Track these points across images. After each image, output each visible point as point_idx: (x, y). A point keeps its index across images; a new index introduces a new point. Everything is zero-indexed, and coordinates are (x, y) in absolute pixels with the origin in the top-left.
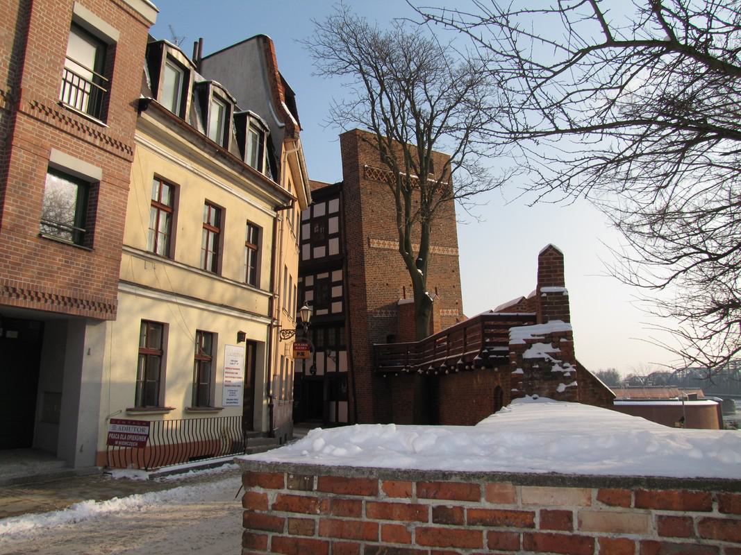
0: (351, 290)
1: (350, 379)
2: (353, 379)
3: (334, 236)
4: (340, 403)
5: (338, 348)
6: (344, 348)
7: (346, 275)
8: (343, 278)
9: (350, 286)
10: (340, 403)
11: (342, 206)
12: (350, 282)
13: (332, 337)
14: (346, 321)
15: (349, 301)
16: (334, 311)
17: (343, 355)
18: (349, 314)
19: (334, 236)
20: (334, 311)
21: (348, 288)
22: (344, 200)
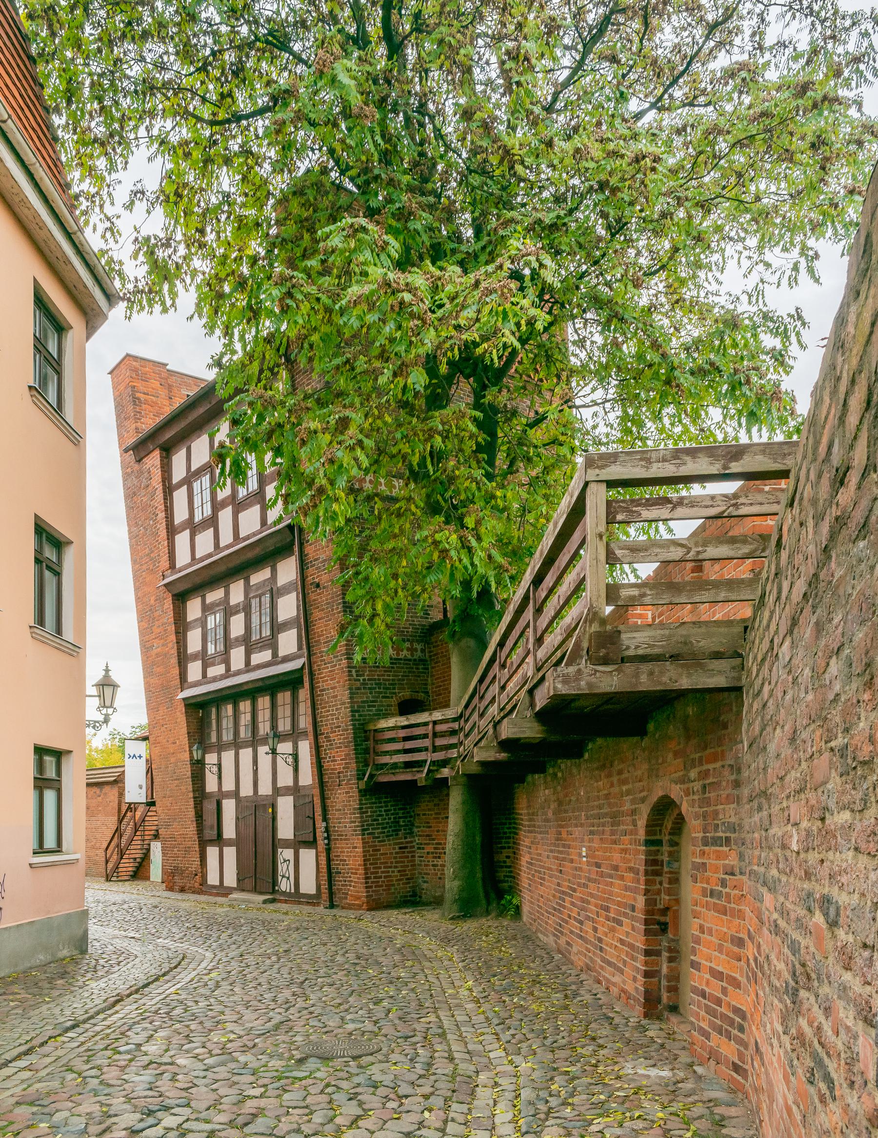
0: (312, 596)
5: (294, 735)
9: (311, 589)
13: (283, 713)
17: (305, 748)
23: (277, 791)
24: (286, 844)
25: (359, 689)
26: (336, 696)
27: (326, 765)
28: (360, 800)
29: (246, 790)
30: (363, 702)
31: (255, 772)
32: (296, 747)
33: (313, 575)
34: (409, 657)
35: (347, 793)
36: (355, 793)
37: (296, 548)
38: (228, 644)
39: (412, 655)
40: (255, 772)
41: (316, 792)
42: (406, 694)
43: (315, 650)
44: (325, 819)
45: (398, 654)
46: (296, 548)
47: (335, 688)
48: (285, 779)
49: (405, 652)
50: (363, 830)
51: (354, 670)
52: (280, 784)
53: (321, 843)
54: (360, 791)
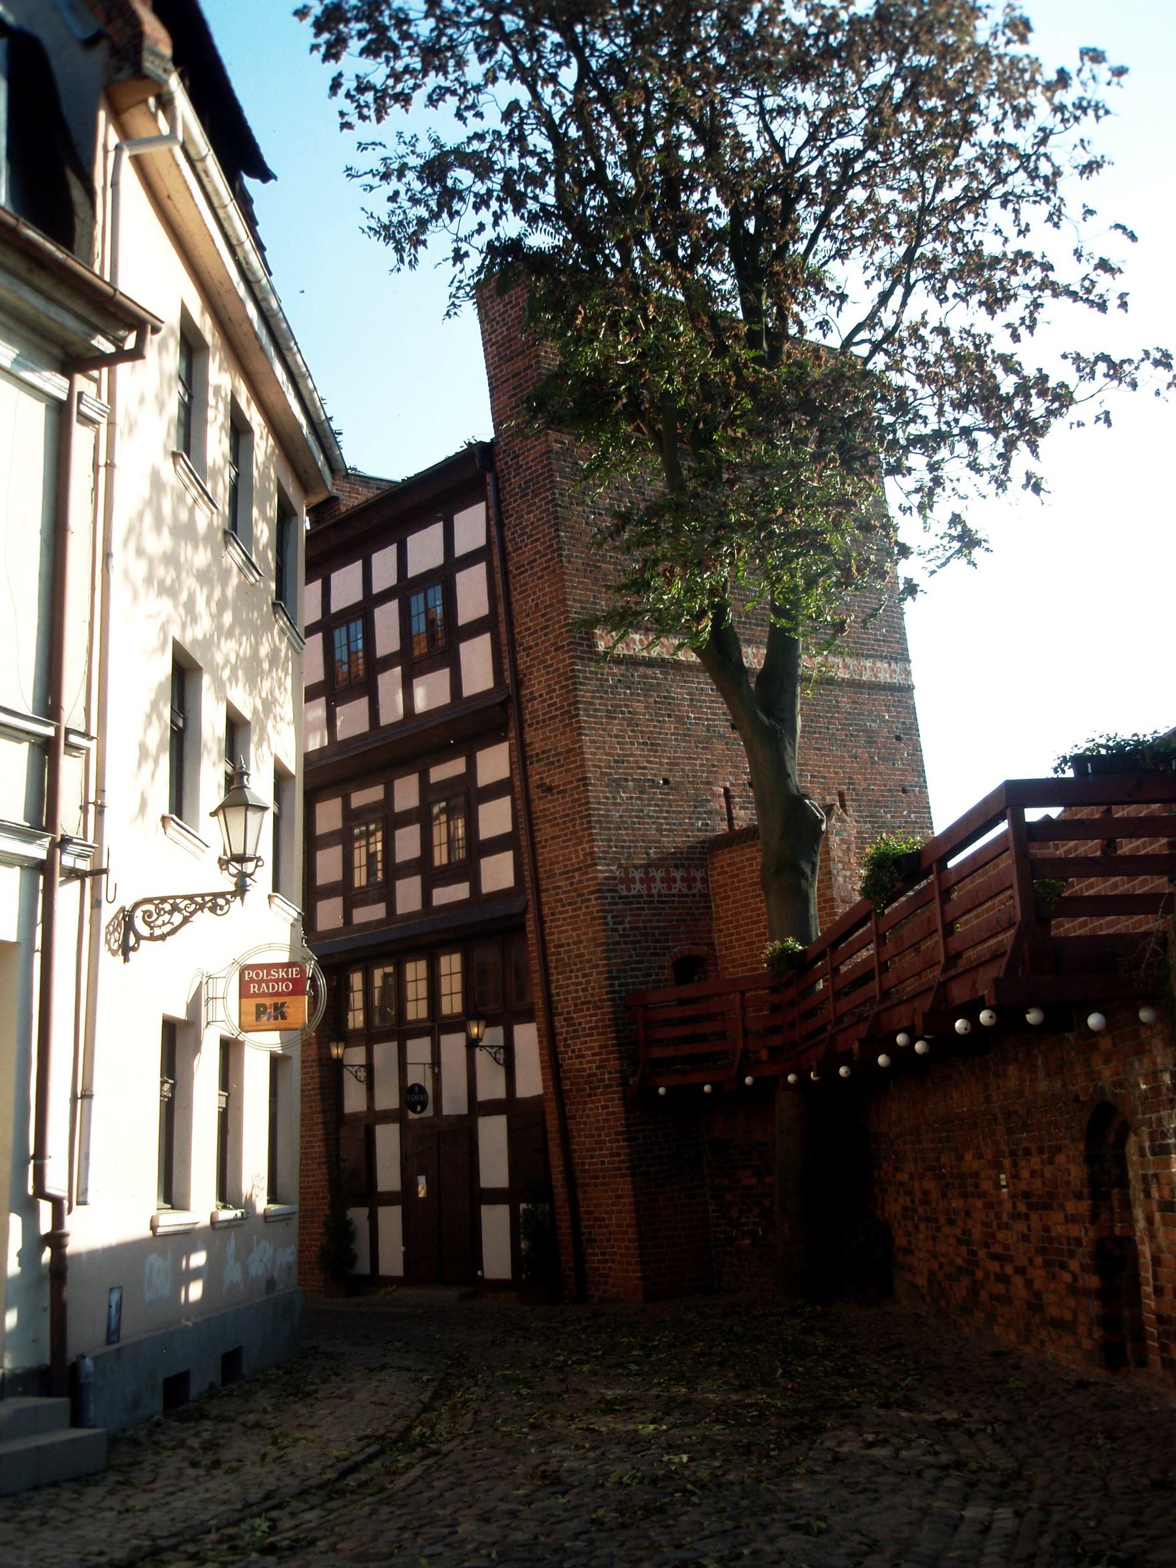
0: (539, 806)
1: (552, 1122)
2: (563, 1118)
3: (475, 629)
6: (527, 1016)
7: (521, 759)
9: (535, 793)
11: (497, 523)
12: (534, 779)
14: (530, 916)
15: (533, 845)
16: (487, 887)
18: (538, 890)
19: (475, 629)
20: (487, 887)
21: (528, 803)
22: (499, 502)
25: (618, 943)
26: (582, 955)
28: (627, 1119)
30: (625, 963)
35: (604, 1107)
36: (616, 1107)
37: (512, 734)
38: (394, 871)
41: (551, 1107)
43: (544, 884)
46: (512, 734)
47: (581, 942)
51: (609, 916)
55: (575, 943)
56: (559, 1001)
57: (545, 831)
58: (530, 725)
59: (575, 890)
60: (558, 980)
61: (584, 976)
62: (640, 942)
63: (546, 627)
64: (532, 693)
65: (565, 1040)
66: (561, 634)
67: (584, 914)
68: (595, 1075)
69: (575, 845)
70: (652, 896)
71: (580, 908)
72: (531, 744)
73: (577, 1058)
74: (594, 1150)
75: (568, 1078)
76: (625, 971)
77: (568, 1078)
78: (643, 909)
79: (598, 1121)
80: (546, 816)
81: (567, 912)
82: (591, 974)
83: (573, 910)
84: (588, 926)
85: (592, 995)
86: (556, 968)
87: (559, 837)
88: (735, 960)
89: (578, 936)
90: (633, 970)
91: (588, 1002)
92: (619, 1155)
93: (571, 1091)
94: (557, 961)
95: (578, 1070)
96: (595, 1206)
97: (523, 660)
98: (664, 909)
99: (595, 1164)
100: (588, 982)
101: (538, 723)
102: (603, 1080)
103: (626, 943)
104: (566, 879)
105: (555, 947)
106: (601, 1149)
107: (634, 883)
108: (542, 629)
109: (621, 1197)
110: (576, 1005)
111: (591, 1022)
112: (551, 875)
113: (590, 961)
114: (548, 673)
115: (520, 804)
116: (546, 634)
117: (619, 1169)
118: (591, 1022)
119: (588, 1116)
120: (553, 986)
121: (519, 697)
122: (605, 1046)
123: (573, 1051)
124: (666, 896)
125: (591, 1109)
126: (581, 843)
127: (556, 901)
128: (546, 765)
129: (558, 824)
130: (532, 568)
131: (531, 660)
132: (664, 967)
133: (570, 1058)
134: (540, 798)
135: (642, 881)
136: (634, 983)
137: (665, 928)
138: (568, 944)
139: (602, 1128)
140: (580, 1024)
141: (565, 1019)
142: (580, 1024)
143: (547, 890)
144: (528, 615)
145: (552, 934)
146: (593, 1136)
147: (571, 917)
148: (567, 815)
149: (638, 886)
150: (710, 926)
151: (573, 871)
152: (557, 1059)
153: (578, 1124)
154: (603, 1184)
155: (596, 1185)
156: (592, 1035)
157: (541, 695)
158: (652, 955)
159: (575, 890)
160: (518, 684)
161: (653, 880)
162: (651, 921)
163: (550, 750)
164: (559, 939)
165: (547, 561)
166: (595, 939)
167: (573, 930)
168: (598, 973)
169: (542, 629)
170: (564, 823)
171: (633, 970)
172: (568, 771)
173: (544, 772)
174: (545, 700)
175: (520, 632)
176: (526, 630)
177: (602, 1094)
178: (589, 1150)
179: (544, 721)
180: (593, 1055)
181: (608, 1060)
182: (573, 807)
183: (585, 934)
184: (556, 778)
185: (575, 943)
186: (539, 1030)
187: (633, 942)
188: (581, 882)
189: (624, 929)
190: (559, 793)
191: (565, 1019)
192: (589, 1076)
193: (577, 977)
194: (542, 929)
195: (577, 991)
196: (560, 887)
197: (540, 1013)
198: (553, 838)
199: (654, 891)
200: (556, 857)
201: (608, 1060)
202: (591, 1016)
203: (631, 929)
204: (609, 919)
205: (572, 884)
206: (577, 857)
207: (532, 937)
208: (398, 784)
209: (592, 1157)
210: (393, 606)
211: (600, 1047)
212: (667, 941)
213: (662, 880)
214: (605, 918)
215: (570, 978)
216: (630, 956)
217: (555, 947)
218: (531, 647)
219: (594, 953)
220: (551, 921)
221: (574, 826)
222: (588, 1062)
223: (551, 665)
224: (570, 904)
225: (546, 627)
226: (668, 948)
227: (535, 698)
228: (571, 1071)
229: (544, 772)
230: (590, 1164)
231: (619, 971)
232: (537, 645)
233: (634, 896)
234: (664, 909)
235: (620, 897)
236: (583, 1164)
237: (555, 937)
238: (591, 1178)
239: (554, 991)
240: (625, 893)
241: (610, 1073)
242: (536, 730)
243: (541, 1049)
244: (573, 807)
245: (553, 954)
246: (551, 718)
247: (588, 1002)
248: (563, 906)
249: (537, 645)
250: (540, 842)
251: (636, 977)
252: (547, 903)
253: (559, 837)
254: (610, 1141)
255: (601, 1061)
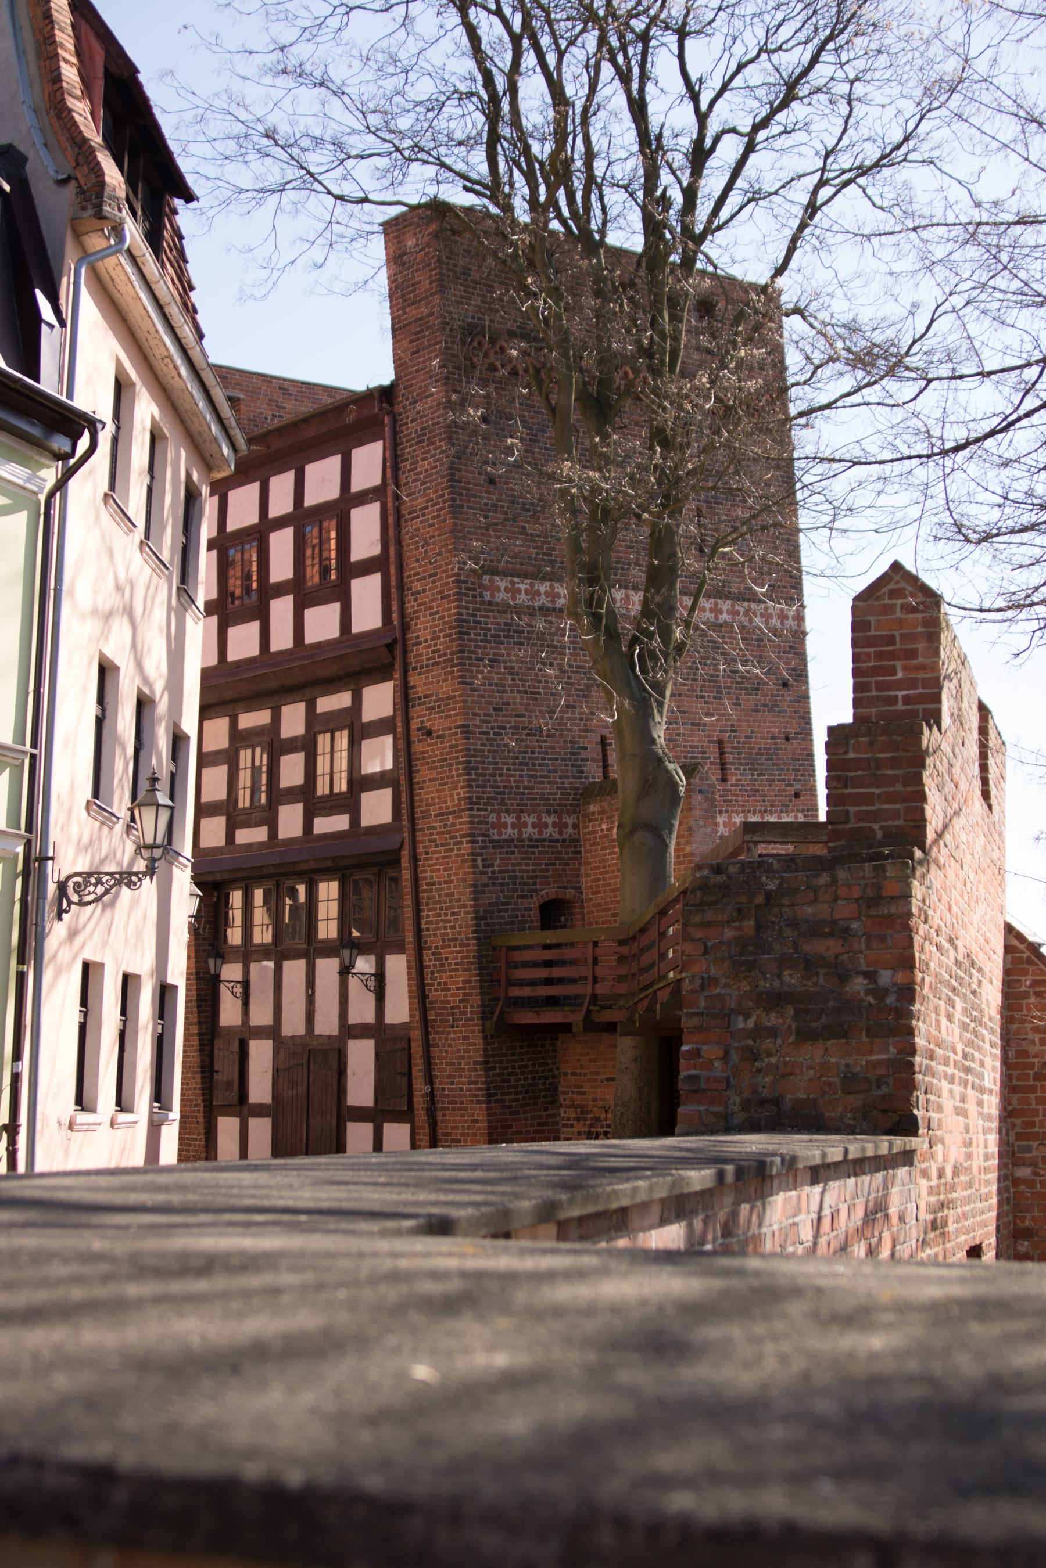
0: (418, 748)
1: (417, 1049)
2: (427, 1046)
3: (366, 567)
4: (387, 1126)
5: (379, 949)
7: (405, 698)
8: (395, 711)
10: (387, 1126)
12: (414, 724)
16: (366, 821)
17: (397, 966)
18: (413, 830)
19: (366, 567)
21: (409, 743)
23: (349, 1031)
24: (361, 1114)
26: (452, 894)
27: (432, 996)
28: (485, 1050)
29: (293, 1025)
31: (311, 999)
32: (381, 965)
33: (419, 716)
34: (556, 836)
39: (560, 833)
40: (311, 999)
41: (416, 1034)
42: (549, 892)
43: (420, 824)
44: (430, 1080)
45: (540, 833)
47: (451, 882)
48: (362, 1011)
49: (550, 829)
50: (489, 1095)
52: (353, 1019)
53: (420, 1114)
54: (485, 1038)
55: (446, 882)
56: (429, 936)
57: (423, 773)
58: (415, 669)
59: (449, 832)
60: (428, 916)
61: (453, 914)
62: (508, 884)
63: (435, 575)
64: (417, 637)
65: (432, 973)
66: (448, 583)
67: (457, 856)
68: (459, 1007)
69: (451, 789)
70: (523, 840)
71: (452, 850)
72: (414, 687)
73: (443, 990)
74: (454, 1077)
75: (433, 1009)
76: (492, 912)
77: (433, 1009)
78: (513, 853)
79: (459, 1051)
80: (424, 758)
81: (440, 852)
82: (459, 913)
83: (446, 851)
84: (459, 868)
85: (460, 933)
86: (427, 904)
87: (436, 779)
88: (599, 905)
89: (449, 876)
90: (500, 911)
91: (456, 939)
92: (476, 1083)
93: (435, 1021)
94: (429, 898)
95: (442, 1002)
96: (453, 1128)
97: (411, 605)
98: (533, 853)
99: (455, 1090)
100: (456, 920)
101: (422, 667)
102: (465, 1013)
103: (494, 884)
104: (441, 821)
105: (428, 884)
106: (461, 1077)
107: (506, 827)
108: (430, 576)
109: (477, 1121)
110: (444, 941)
111: (456, 958)
112: (426, 815)
113: (458, 900)
114: (434, 620)
115: (401, 745)
116: (434, 582)
117: (477, 1096)
118: (456, 958)
119: (450, 1046)
120: (423, 921)
121: (404, 640)
122: (470, 982)
123: (439, 984)
124: (537, 840)
125: (453, 1039)
126: (456, 788)
127: (431, 841)
128: (428, 709)
129: (436, 768)
130: (424, 515)
131: (419, 605)
132: (530, 909)
133: (436, 990)
134: (420, 741)
135: (513, 826)
136: (500, 924)
137: (534, 871)
138: (440, 883)
139: (463, 1058)
140: (447, 959)
141: (433, 954)
142: (447, 959)
143: (422, 829)
144: (417, 561)
145: (425, 871)
146: (453, 1064)
147: (443, 858)
148: (445, 760)
149: (510, 830)
150: (579, 870)
151: (450, 813)
152: (424, 991)
153: (441, 1051)
154: (460, 1109)
155: (454, 1109)
156: (457, 970)
157: (426, 641)
158: (519, 897)
159: (449, 832)
160: (405, 628)
161: (525, 825)
162: (520, 864)
163: (431, 696)
164: (431, 877)
165: (439, 510)
166: (464, 880)
167: (445, 870)
168: (466, 913)
169: (430, 576)
170: (442, 767)
171: (500, 911)
172: (447, 717)
173: (424, 715)
174: (429, 646)
175: (409, 576)
176: (415, 575)
177: (464, 1026)
178: (448, 1077)
179: (427, 666)
180: (458, 989)
181: (471, 994)
182: (451, 753)
183: (455, 874)
184: (437, 724)
185: (446, 882)
186: (408, 961)
187: (502, 885)
188: (454, 825)
189: (493, 872)
190: (438, 737)
191: (433, 954)
192: (452, 1008)
193: (446, 915)
194: (416, 867)
195: (445, 928)
196: (435, 828)
197: (410, 947)
198: (430, 780)
199: (525, 836)
200: (433, 798)
201: (471, 994)
202: (457, 952)
203: (500, 872)
204: (479, 862)
205: (445, 826)
206: (453, 800)
207: (406, 874)
208: (285, 710)
209: (452, 1083)
210: (288, 533)
211: (464, 982)
212: (535, 884)
213: (534, 826)
214: (474, 861)
215: (440, 915)
216: (498, 897)
217: (428, 884)
218: (419, 593)
219: (462, 893)
220: (426, 859)
221: (450, 770)
222: (453, 995)
223: (437, 613)
224: (442, 845)
225: (435, 575)
226: (536, 891)
227: (420, 643)
228: (436, 1002)
229: (424, 715)
230: (450, 1090)
231: (485, 911)
232: (424, 591)
233: (504, 840)
234: (533, 853)
235: (491, 841)
236: (443, 1089)
237: (428, 875)
238: (449, 1102)
239: (424, 926)
240: (496, 837)
241: (472, 1007)
242: (420, 674)
243: (409, 979)
244: (451, 753)
245: (425, 891)
246: (433, 664)
247: (456, 939)
248: (436, 846)
249: (424, 591)
250: (418, 783)
251: (502, 917)
252: (422, 842)
253: (436, 779)
254: (469, 1070)
255: (464, 995)
